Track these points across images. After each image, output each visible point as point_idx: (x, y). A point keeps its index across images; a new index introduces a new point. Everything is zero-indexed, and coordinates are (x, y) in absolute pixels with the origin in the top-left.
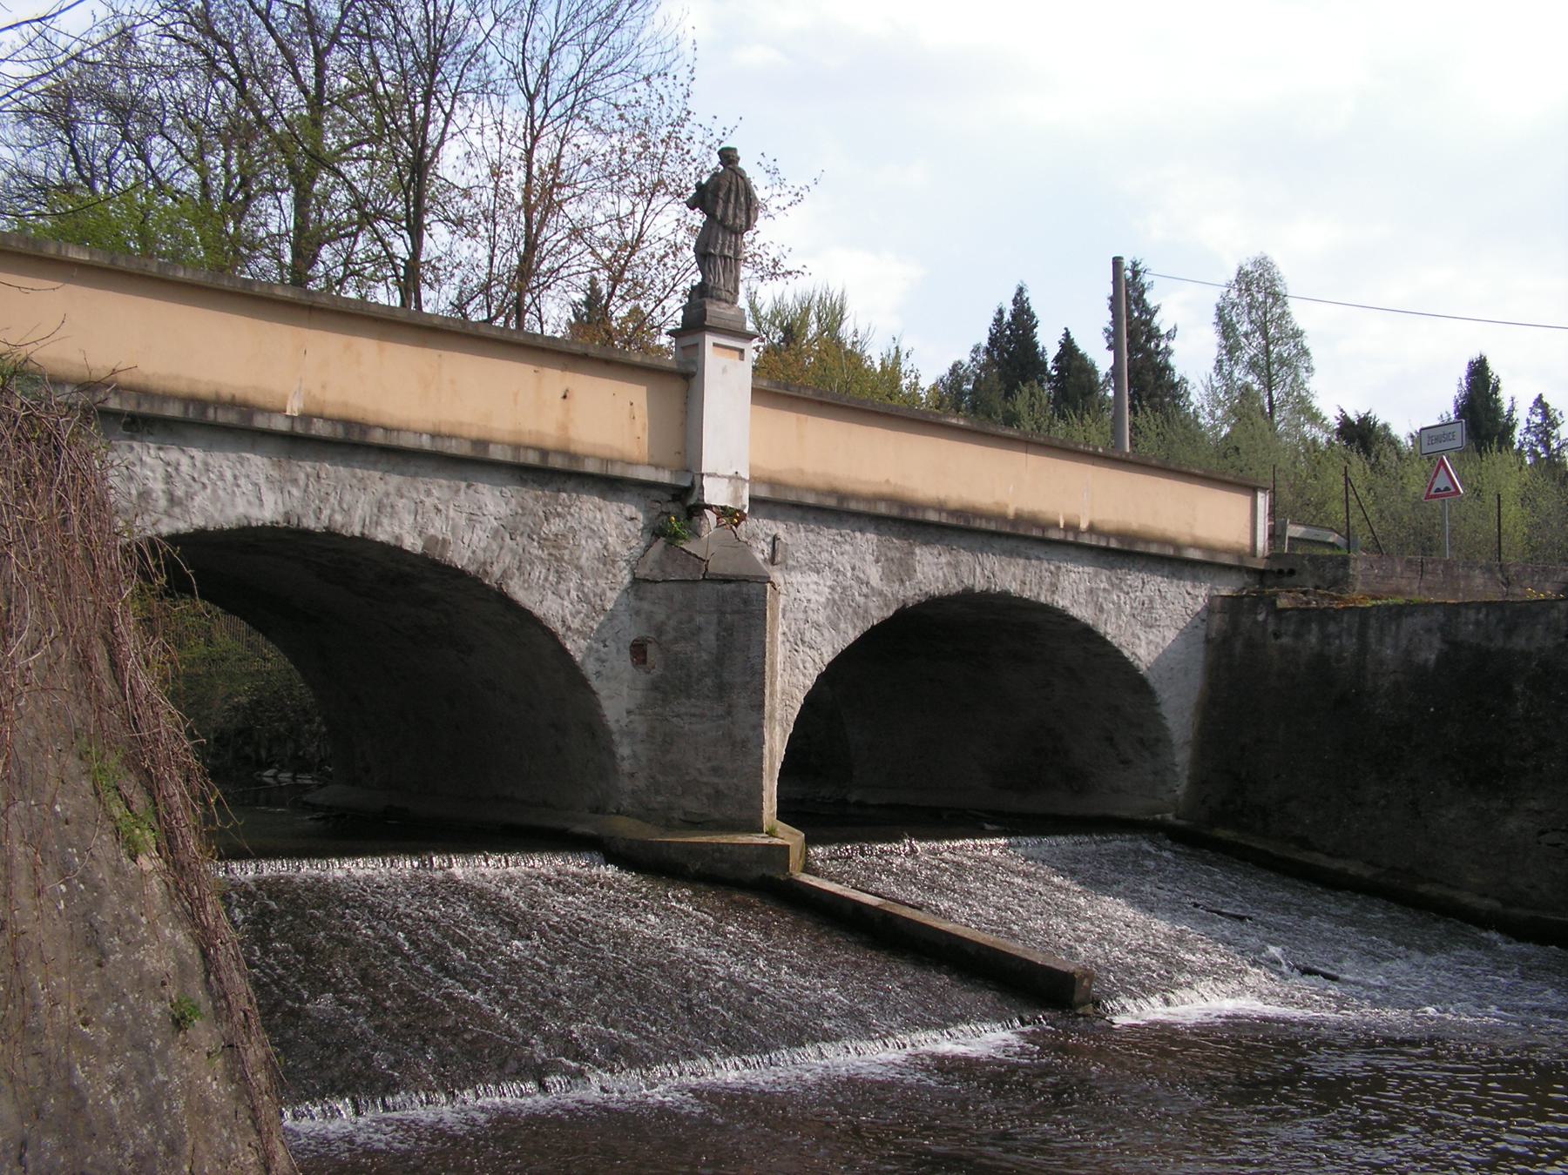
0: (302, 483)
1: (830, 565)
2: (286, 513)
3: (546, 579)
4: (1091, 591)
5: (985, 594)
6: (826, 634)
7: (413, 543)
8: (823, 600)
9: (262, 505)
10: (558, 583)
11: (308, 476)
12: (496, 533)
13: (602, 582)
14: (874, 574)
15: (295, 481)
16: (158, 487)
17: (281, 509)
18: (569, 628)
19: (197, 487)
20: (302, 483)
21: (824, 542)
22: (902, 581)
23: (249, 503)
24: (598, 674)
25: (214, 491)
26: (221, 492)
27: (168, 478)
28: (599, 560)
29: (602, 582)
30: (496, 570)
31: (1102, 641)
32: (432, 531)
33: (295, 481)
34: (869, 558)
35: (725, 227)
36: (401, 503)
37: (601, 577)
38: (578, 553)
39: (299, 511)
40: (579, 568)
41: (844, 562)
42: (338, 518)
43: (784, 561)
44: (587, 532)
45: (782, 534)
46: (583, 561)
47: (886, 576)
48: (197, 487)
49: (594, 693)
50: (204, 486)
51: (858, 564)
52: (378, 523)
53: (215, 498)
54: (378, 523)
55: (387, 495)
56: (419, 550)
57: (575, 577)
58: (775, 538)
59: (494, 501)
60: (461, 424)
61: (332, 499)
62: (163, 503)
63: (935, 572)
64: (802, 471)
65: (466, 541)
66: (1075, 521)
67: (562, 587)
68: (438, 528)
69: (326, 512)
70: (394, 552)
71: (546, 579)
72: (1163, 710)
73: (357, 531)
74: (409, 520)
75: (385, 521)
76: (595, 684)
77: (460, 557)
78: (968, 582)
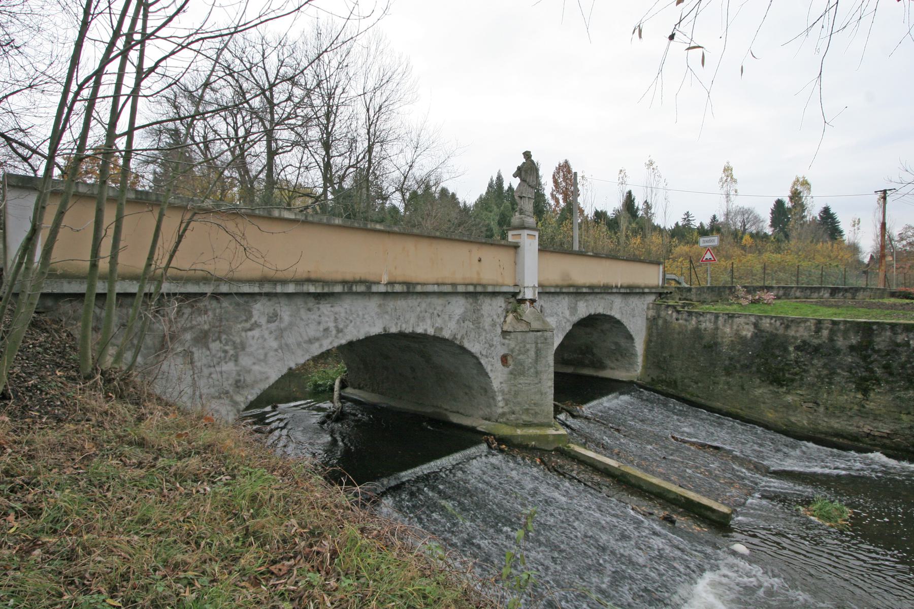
5: (595, 315)
7: (431, 331)
14: (567, 313)
16: (331, 325)
19: (348, 322)
21: (554, 305)
23: (370, 325)
27: (336, 320)
30: (459, 337)
31: (622, 324)
42: (404, 326)
46: (486, 327)
48: (348, 322)
56: (432, 334)
57: (484, 334)
62: (334, 332)
63: (584, 309)
68: (439, 322)
74: (429, 322)
76: (490, 374)
77: (446, 334)
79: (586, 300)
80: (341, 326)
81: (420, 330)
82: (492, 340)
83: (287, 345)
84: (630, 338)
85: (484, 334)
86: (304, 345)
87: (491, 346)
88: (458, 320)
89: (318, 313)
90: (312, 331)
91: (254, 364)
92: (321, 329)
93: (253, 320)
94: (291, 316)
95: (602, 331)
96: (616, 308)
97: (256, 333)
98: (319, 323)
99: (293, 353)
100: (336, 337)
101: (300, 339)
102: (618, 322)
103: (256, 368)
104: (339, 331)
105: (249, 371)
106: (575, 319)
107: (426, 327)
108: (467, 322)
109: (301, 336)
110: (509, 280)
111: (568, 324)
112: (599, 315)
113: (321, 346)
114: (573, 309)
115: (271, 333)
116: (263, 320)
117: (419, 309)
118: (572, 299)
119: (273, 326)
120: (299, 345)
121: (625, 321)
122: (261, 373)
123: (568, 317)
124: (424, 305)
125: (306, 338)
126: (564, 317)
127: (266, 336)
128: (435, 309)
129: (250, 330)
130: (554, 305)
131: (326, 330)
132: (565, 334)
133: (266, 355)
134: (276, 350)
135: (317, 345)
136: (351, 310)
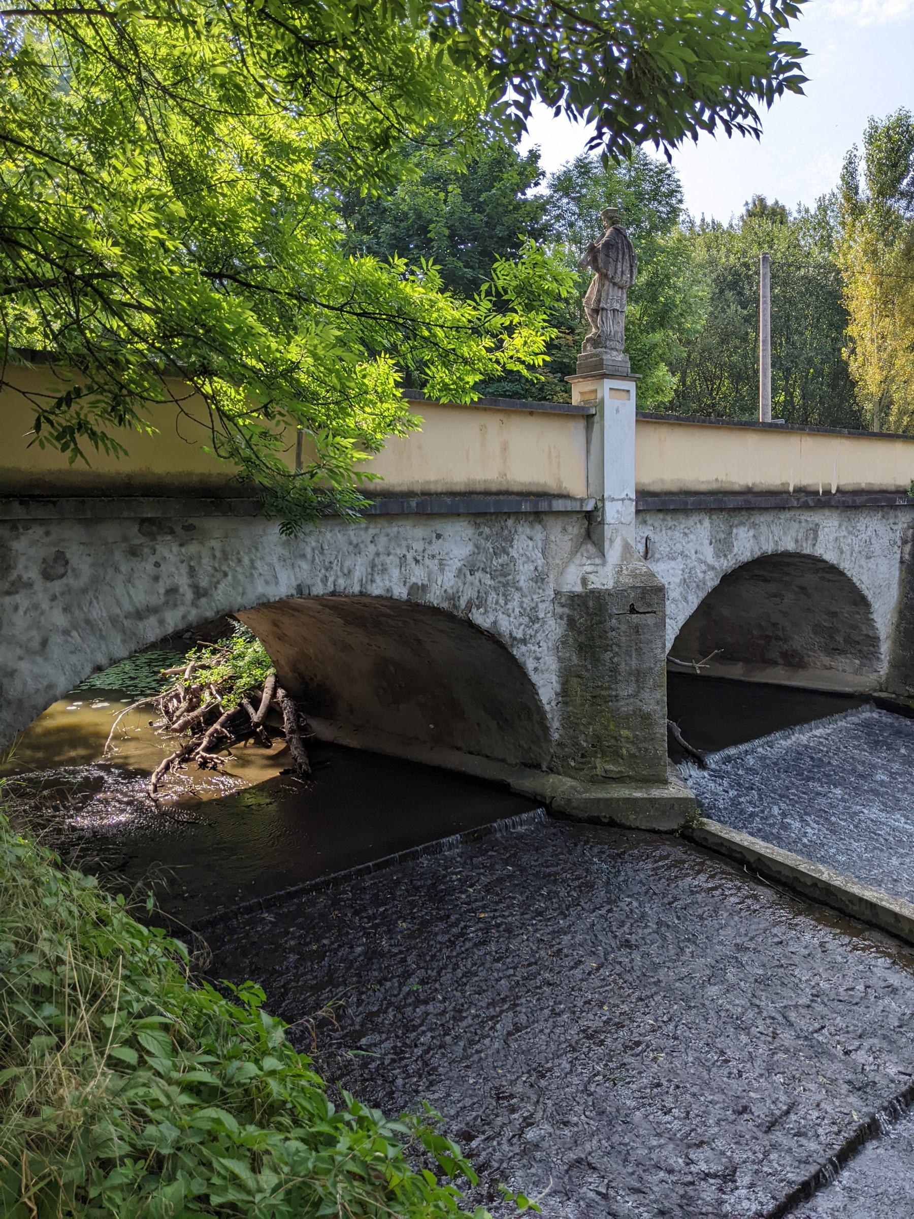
0: (309, 556)
1: (682, 553)
2: (299, 586)
3: (497, 603)
4: (836, 539)
5: (775, 555)
6: (680, 606)
7: (400, 592)
8: (678, 581)
9: (277, 583)
10: (506, 604)
11: (313, 550)
12: (460, 573)
13: (535, 597)
14: (708, 553)
15: (304, 556)
16: (183, 582)
17: (295, 584)
18: (515, 639)
19: (219, 575)
20: (309, 556)
21: (677, 535)
22: (725, 556)
23: (267, 582)
24: (536, 669)
25: (234, 577)
26: (241, 577)
27: (192, 572)
28: (532, 579)
29: (535, 597)
30: (463, 603)
32: (413, 580)
33: (304, 556)
34: (707, 542)
35: (614, 284)
36: (388, 560)
37: (535, 593)
38: (517, 578)
39: (309, 582)
40: (518, 589)
41: (690, 549)
42: (341, 582)
43: (653, 556)
44: (524, 559)
45: (651, 536)
46: (522, 584)
47: (717, 556)
48: (219, 575)
49: (533, 685)
50: (226, 575)
51: (699, 549)
52: (372, 581)
53: (236, 583)
54: (372, 581)
55: (378, 554)
56: (405, 596)
57: (517, 596)
58: (647, 538)
59: (458, 542)
60: (429, 482)
61: (334, 566)
62: (189, 596)
63: (748, 542)
64: (662, 481)
65: (439, 583)
66: (827, 488)
67: (509, 606)
68: (418, 575)
69: (331, 579)
70: (388, 600)
71: (497, 603)
72: (874, 616)
73: (759, 554)
74: (395, 573)
75: (378, 578)
76: (534, 677)
77: (434, 597)
78: (764, 548)
79: (754, 525)
80: (204, 583)
81: (376, 590)
82: (535, 609)
83: (88, 622)
84: (861, 602)
85: (517, 596)
86: (127, 623)
87: (534, 620)
88: (460, 570)
89: (153, 559)
90: (141, 593)
91: (21, 658)
92: (162, 591)
93: (14, 575)
94: (93, 565)
95: (802, 589)
96: (832, 540)
97: (21, 599)
98: (156, 579)
99: (102, 637)
100: (193, 604)
101: (118, 611)
102: (833, 569)
103: (24, 666)
104: (199, 593)
105: (12, 674)
106: (727, 564)
107: (393, 584)
108: (479, 574)
109: (118, 603)
110: (576, 485)
111: (711, 574)
112: (786, 554)
113: (161, 622)
114: (723, 545)
115: (54, 598)
116: (33, 574)
117: (372, 549)
118: (720, 520)
119: (56, 586)
120: (114, 620)
121: (845, 566)
122: (36, 677)
123: (710, 560)
124: (383, 541)
125: (128, 607)
126: (701, 562)
127: (45, 606)
128: (409, 548)
129: (8, 593)
130: (677, 535)
131: (172, 591)
132: (702, 595)
133: (44, 643)
134: (66, 632)
135: (152, 620)
136: (224, 552)
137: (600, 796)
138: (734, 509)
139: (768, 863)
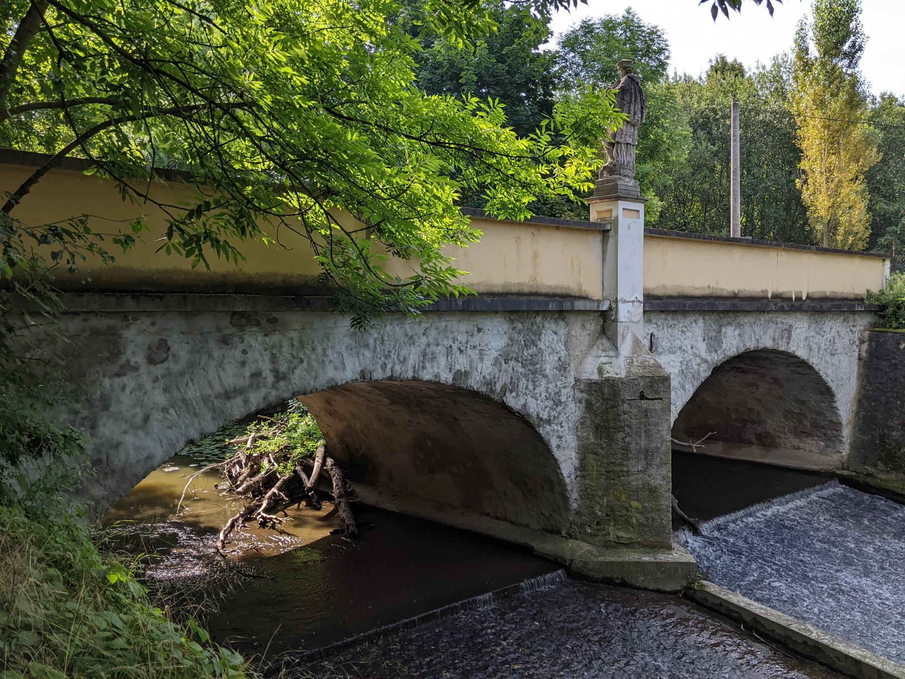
0: (372, 346)
1: (680, 348)
2: (362, 371)
4: (806, 338)
5: (756, 351)
6: (679, 393)
7: (447, 377)
8: (677, 371)
9: (344, 369)
10: (534, 389)
11: (375, 340)
12: (496, 362)
13: (559, 383)
14: (702, 347)
16: (266, 367)
17: (359, 370)
18: (541, 419)
19: (296, 362)
20: (372, 346)
21: (677, 332)
22: (716, 351)
23: (336, 368)
24: (558, 446)
25: (309, 363)
26: (314, 363)
27: (274, 358)
28: (556, 368)
29: (559, 383)
30: (498, 388)
31: (811, 368)
32: (458, 367)
36: (437, 350)
38: (544, 366)
39: (371, 368)
40: (545, 376)
41: (687, 344)
42: (398, 368)
43: (656, 350)
44: (550, 350)
45: (655, 333)
46: (548, 372)
48: (296, 362)
49: (556, 460)
50: (302, 361)
51: (694, 344)
52: (424, 368)
53: (310, 369)
54: (424, 368)
55: (428, 345)
56: (450, 381)
57: (543, 382)
58: (652, 335)
59: (495, 336)
61: (392, 354)
62: (270, 379)
63: (736, 339)
64: (664, 286)
65: (479, 370)
68: (462, 363)
69: (389, 366)
70: (436, 385)
71: (527, 388)
72: (838, 405)
74: (442, 360)
75: (428, 365)
76: (557, 454)
77: (474, 382)
78: (748, 345)
79: (739, 326)
80: (283, 368)
81: (427, 375)
82: (558, 393)
83: (184, 400)
84: (826, 392)
85: (543, 382)
86: (217, 402)
87: (558, 403)
88: (497, 359)
89: (241, 347)
90: (230, 377)
91: (125, 432)
92: (247, 374)
93: (123, 360)
94: (191, 352)
95: (775, 380)
96: (802, 339)
97: (128, 381)
98: (243, 364)
99: (196, 415)
100: (274, 386)
101: (209, 392)
102: (804, 365)
103: (128, 439)
104: (279, 376)
105: (117, 446)
106: (717, 358)
107: (440, 371)
108: (512, 363)
109: (210, 385)
110: (593, 289)
111: (704, 366)
112: (765, 350)
113: (246, 402)
114: (714, 342)
115: (156, 380)
116: (139, 359)
117: (424, 340)
118: (711, 319)
119: (159, 370)
120: (206, 400)
121: (814, 361)
122: (138, 449)
123: (704, 354)
124: (433, 333)
125: (218, 388)
126: (696, 355)
127: (148, 386)
128: (454, 340)
129: (118, 375)
130: (677, 332)
131: (256, 375)
132: (697, 384)
133: (146, 419)
134: (165, 410)
135: (239, 400)
136: (301, 343)
137: (613, 559)
138: (723, 312)
139: (762, 622)
